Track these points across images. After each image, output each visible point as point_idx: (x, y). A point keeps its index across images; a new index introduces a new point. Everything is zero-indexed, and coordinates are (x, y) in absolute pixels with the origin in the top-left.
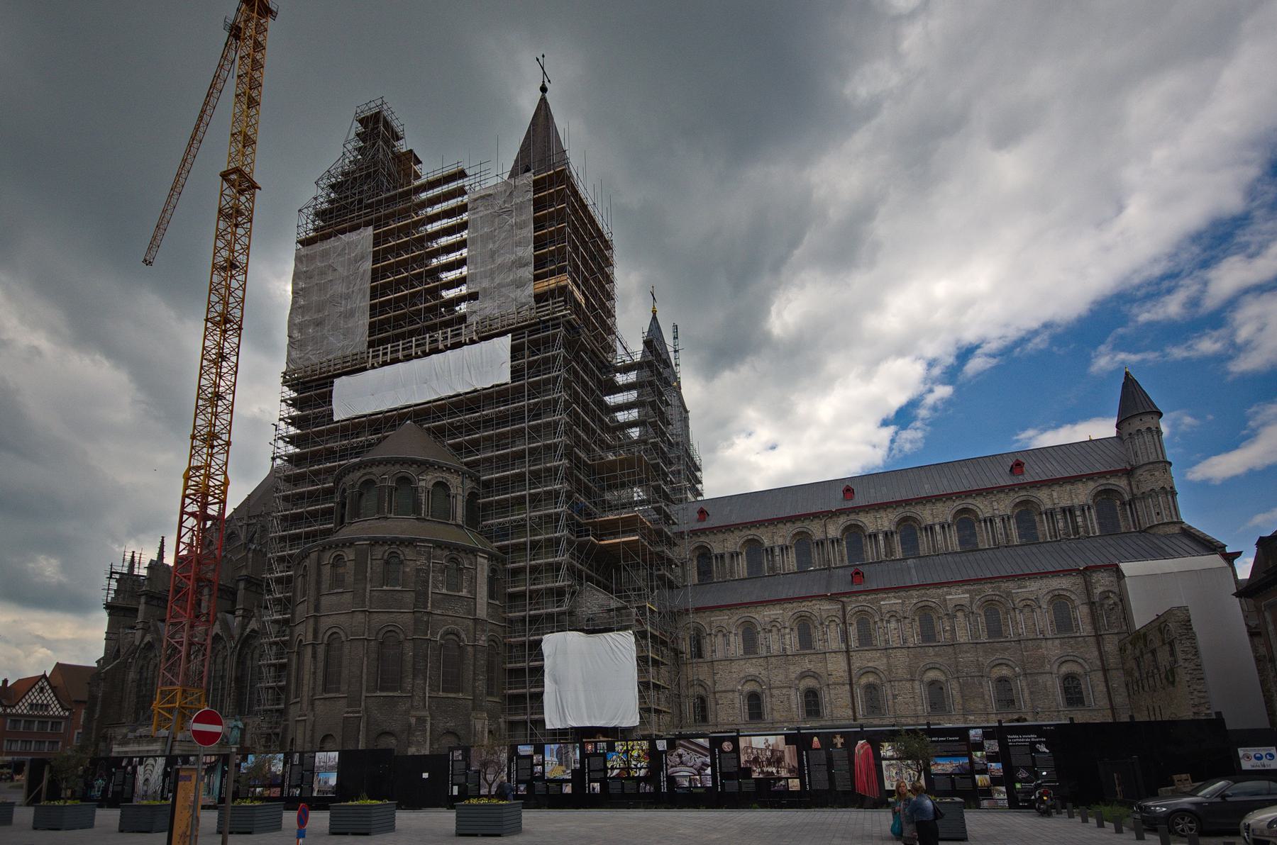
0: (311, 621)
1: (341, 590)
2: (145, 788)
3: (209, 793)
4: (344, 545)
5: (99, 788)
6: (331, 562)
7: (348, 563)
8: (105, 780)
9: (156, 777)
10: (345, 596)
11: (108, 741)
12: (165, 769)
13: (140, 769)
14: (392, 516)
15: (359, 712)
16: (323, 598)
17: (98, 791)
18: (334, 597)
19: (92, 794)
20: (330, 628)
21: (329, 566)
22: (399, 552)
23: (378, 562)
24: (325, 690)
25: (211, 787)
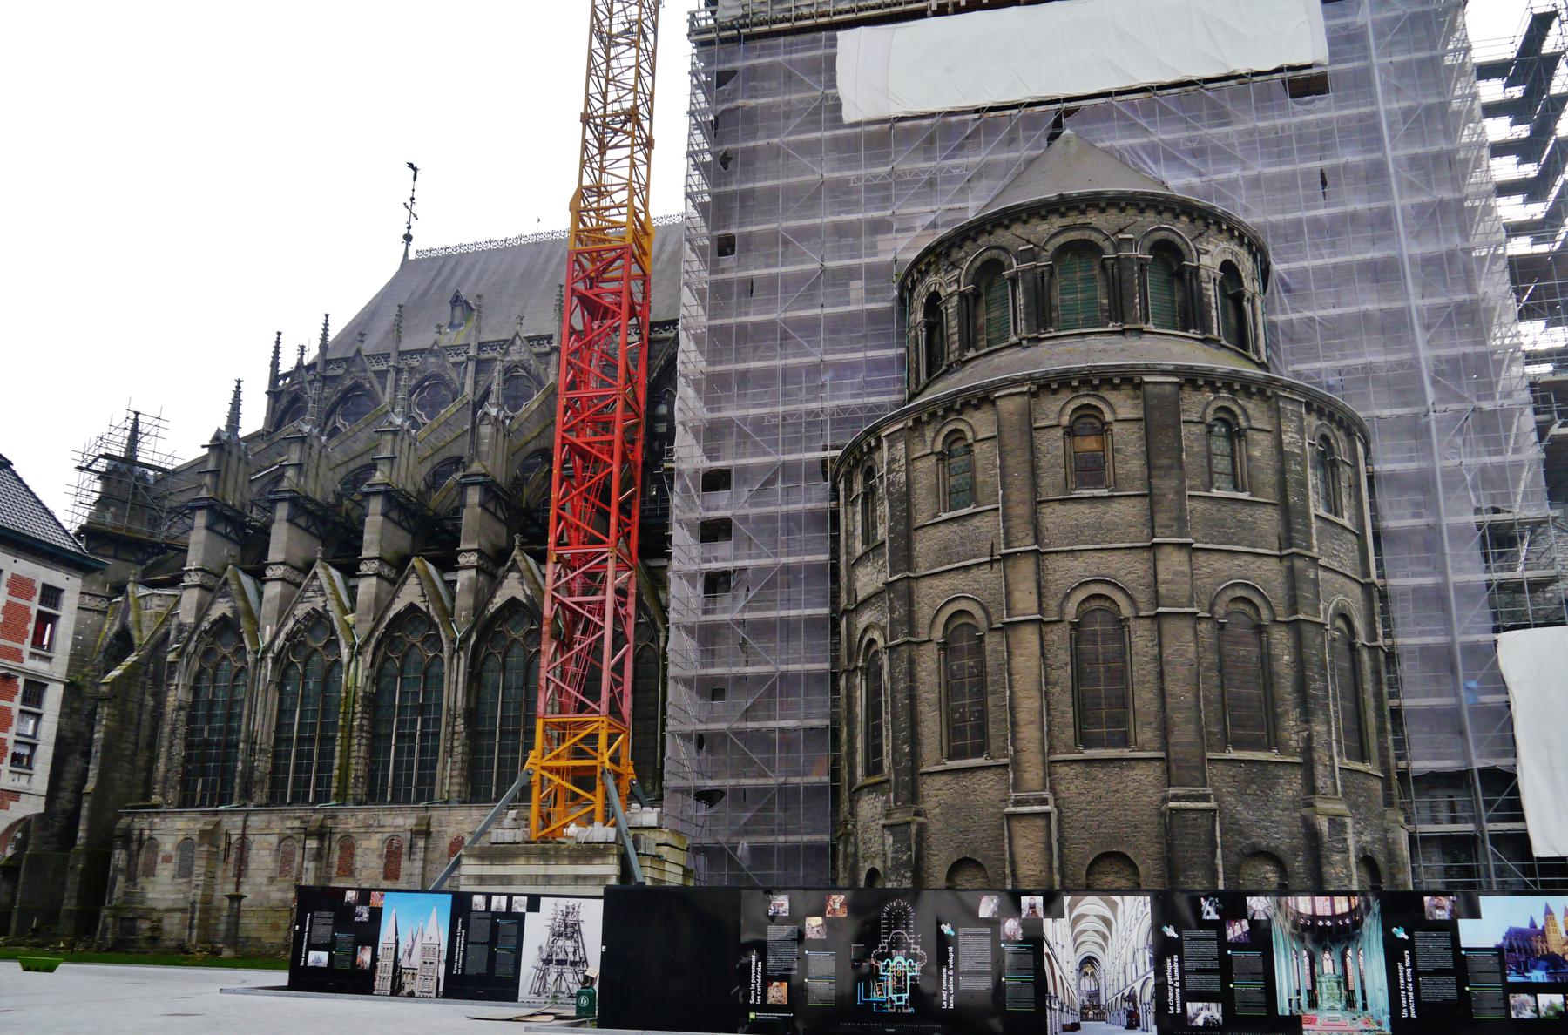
0: (1027, 567)
1: (1104, 492)
2: (1088, 984)
3: (1350, 1004)
4: (966, 405)
5: (900, 980)
6: (1065, 420)
7: (977, 448)
8: (915, 958)
9: (1127, 955)
10: (1115, 506)
11: (134, 847)
12: (1157, 928)
13: (1056, 932)
14: (1150, 327)
15: (1205, 798)
16: (1046, 510)
17: (898, 990)
18: (1085, 509)
19: (875, 997)
20: (1081, 584)
21: (1059, 432)
22: (1235, 408)
23: (1193, 428)
24: (1085, 741)
25: (1354, 984)
